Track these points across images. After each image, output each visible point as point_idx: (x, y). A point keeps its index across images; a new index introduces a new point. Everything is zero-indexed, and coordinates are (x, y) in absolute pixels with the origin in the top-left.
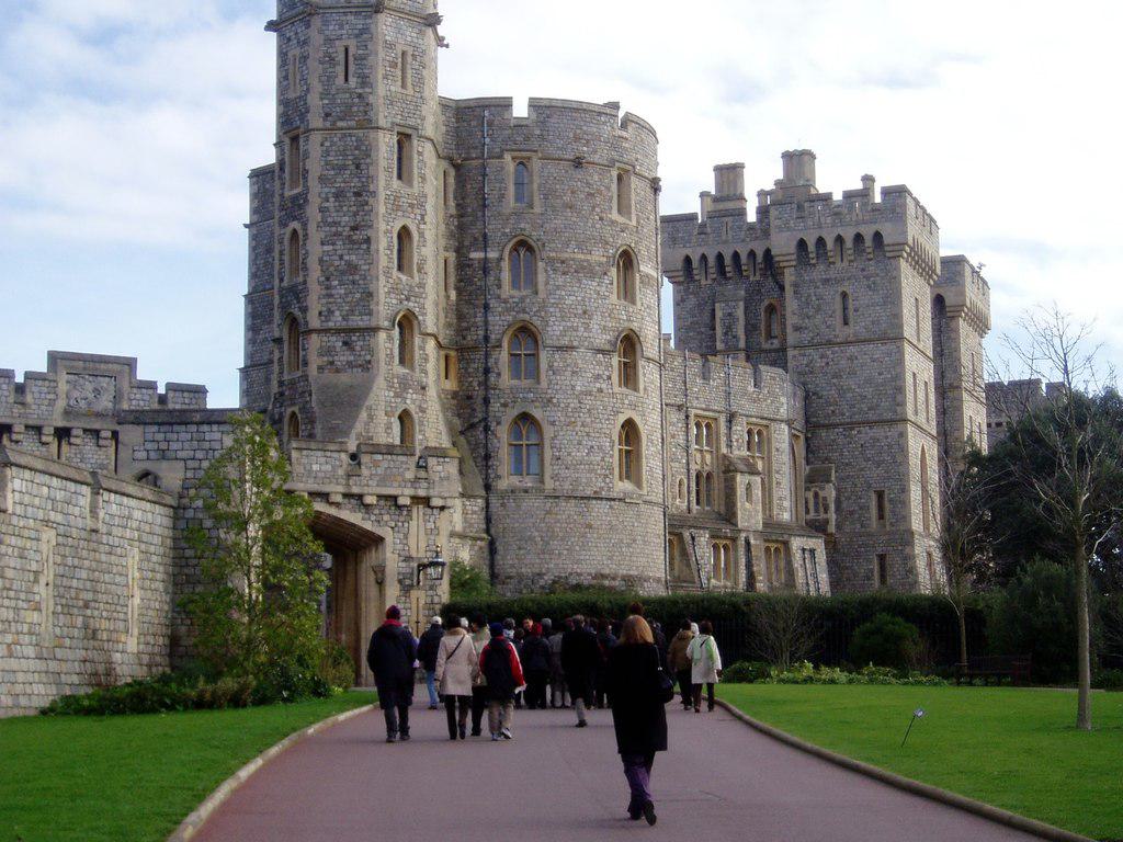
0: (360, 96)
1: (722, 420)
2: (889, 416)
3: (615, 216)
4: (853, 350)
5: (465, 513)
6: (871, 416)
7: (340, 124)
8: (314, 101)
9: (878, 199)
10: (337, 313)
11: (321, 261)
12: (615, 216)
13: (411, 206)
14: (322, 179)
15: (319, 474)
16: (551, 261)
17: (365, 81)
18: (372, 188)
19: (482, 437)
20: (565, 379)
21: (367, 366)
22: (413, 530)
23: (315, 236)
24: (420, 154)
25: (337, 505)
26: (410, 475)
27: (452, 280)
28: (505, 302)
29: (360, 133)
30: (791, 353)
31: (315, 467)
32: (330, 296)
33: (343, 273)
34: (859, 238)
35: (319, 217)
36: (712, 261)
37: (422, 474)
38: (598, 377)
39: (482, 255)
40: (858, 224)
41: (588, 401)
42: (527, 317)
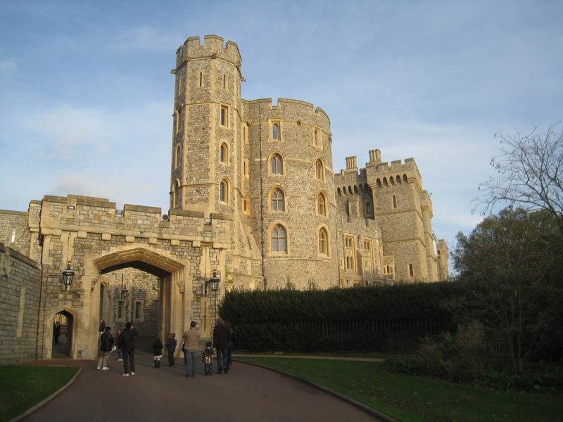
1: (355, 237)
3: (314, 145)
4: (398, 215)
5: (252, 267)
7: (197, 102)
8: (188, 93)
9: (403, 163)
12: (314, 145)
13: (227, 135)
15: (142, 226)
16: (288, 161)
17: (208, 84)
18: (210, 126)
19: (260, 234)
21: (206, 201)
22: (203, 262)
23: (186, 146)
24: (232, 114)
25: (155, 245)
26: (200, 229)
27: (247, 170)
28: (270, 178)
30: (376, 217)
31: (140, 222)
35: (188, 139)
36: (347, 189)
37: (208, 228)
38: (309, 209)
41: (306, 219)
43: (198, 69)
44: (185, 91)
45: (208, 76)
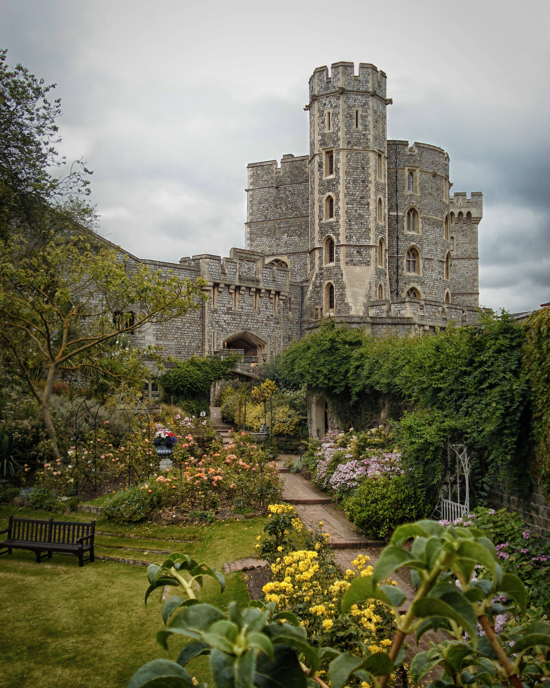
0: (364, 135)
2: (471, 291)
6: (463, 291)
7: (355, 147)
9: (469, 197)
10: (354, 237)
11: (347, 212)
14: (347, 173)
17: (366, 127)
18: (370, 179)
20: (428, 273)
29: (364, 152)
32: (351, 229)
33: (357, 219)
34: (460, 214)
39: (396, 214)
40: (461, 207)
42: (414, 243)
43: (354, 106)
44: (339, 130)
45: (366, 117)
